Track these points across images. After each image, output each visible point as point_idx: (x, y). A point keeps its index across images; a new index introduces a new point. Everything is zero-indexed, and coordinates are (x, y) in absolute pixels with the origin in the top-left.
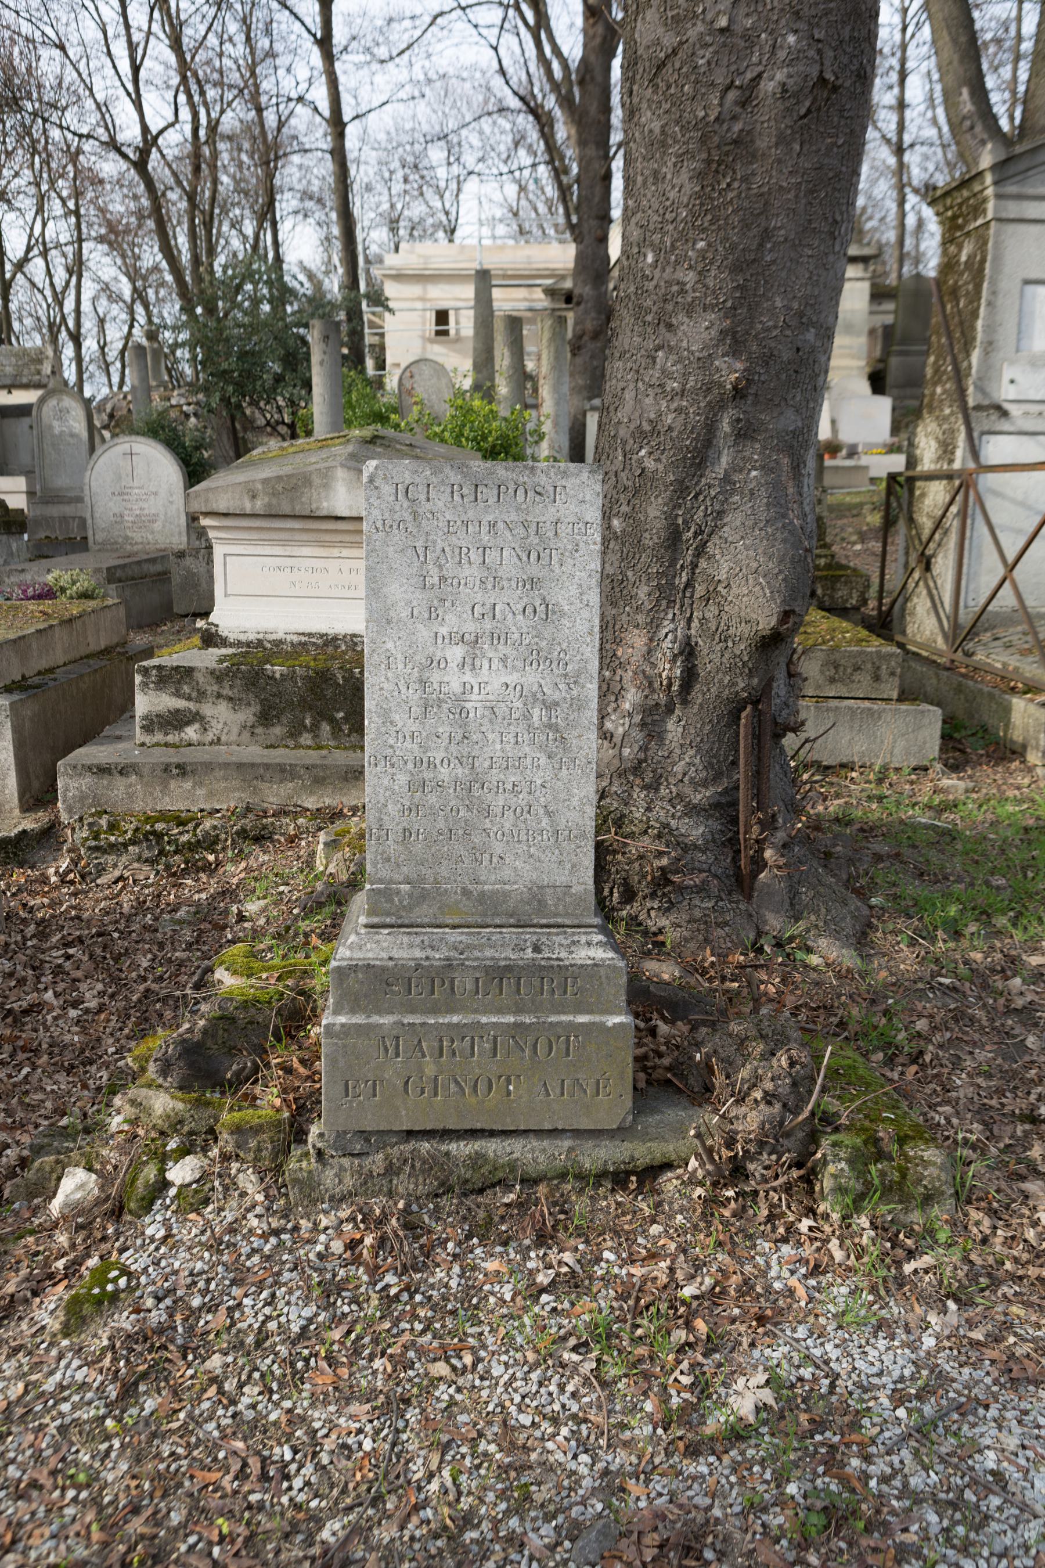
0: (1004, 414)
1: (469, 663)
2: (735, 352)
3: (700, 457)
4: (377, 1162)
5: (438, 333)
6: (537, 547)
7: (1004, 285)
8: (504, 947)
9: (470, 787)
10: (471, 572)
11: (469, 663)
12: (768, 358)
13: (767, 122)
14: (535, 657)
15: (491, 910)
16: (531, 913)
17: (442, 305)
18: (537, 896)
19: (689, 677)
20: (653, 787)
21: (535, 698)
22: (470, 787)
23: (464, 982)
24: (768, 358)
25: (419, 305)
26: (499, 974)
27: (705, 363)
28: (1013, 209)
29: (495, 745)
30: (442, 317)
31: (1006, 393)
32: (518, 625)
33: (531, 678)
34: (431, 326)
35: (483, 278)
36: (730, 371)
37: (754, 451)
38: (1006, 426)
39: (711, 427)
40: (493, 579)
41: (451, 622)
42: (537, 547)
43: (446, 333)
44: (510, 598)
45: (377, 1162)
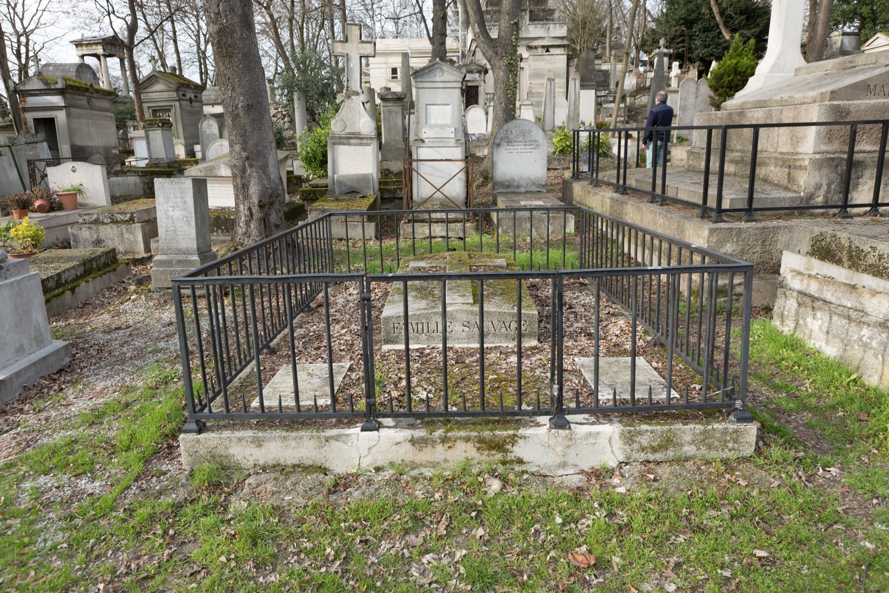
0: (423, 141)
1: (173, 211)
2: (245, 151)
3: (244, 171)
4: (162, 293)
5: (393, 78)
6: (182, 192)
7: (420, 106)
8: (181, 257)
9: (175, 231)
10: (172, 196)
11: (173, 211)
12: (251, 152)
13: (241, 112)
14: (184, 209)
15: (180, 251)
16: (186, 252)
17: (394, 66)
18: (187, 249)
19: (251, 214)
20: (249, 237)
21: (184, 216)
22: (175, 231)
23: (174, 263)
24: (251, 152)
25: (384, 66)
26: (179, 262)
27: (240, 153)
28: (421, 85)
29: (178, 224)
30: (394, 71)
31: (424, 136)
32: (180, 204)
33: (183, 213)
34: (389, 74)
35: (405, 56)
36: (244, 154)
37: (254, 169)
38: (423, 145)
39: (244, 165)
40: (176, 197)
41: (170, 204)
42: (182, 192)
43: (396, 78)
44: (179, 200)
45: (162, 293)
